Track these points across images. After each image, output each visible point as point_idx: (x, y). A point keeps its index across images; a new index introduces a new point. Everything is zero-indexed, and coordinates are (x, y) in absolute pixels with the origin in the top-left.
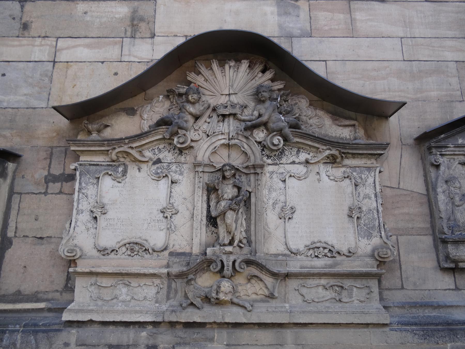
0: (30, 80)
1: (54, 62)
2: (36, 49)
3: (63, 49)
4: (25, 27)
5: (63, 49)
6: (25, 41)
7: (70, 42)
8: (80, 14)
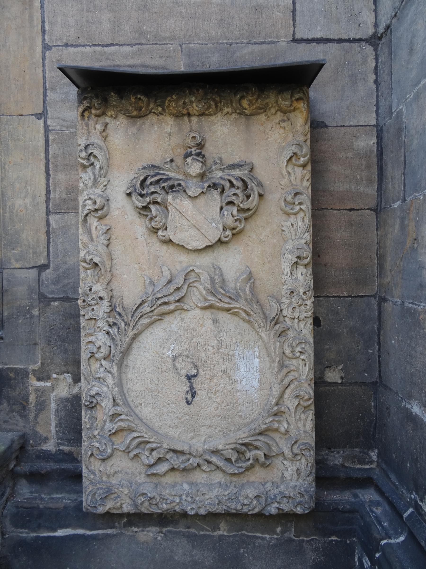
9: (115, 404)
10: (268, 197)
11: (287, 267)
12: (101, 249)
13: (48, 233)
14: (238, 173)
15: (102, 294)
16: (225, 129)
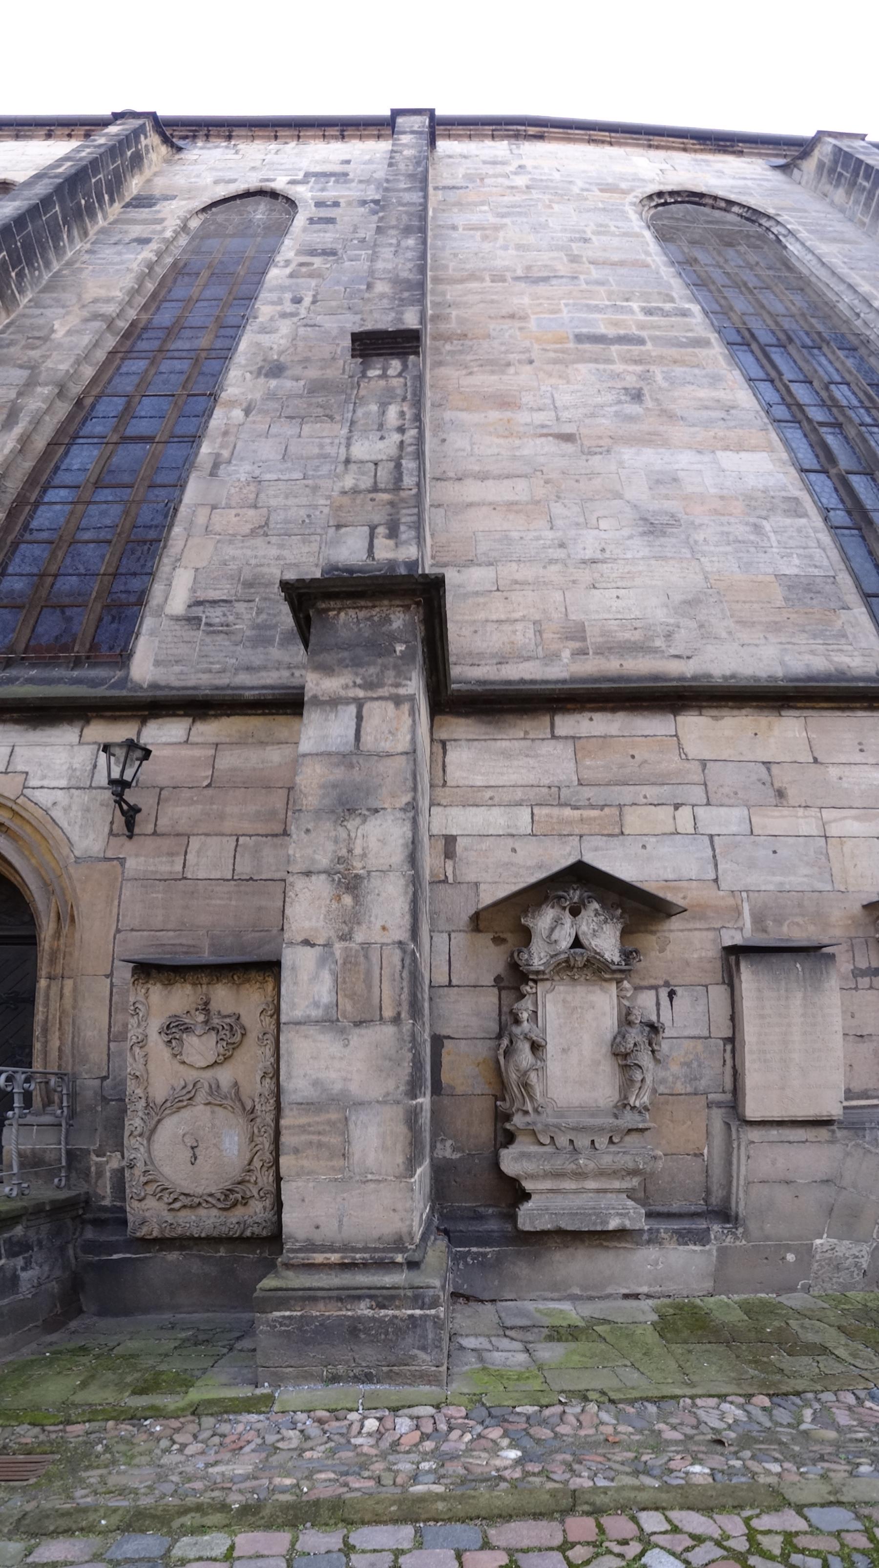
0: (805, 858)
1: (826, 837)
2: (801, 821)
3: (830, 822)
4: (781, 794)
5: (830, 822)
6: (786, 811)
7: (835, 813)
8: (835, 779)
9: (146, 1164)
10: (249, 1034)
11: (258, 1079)
12: (141, 1067)
13: (109, 1055)
14: (228, 1020)
15: (141, 1095)
16: (223, 993)
